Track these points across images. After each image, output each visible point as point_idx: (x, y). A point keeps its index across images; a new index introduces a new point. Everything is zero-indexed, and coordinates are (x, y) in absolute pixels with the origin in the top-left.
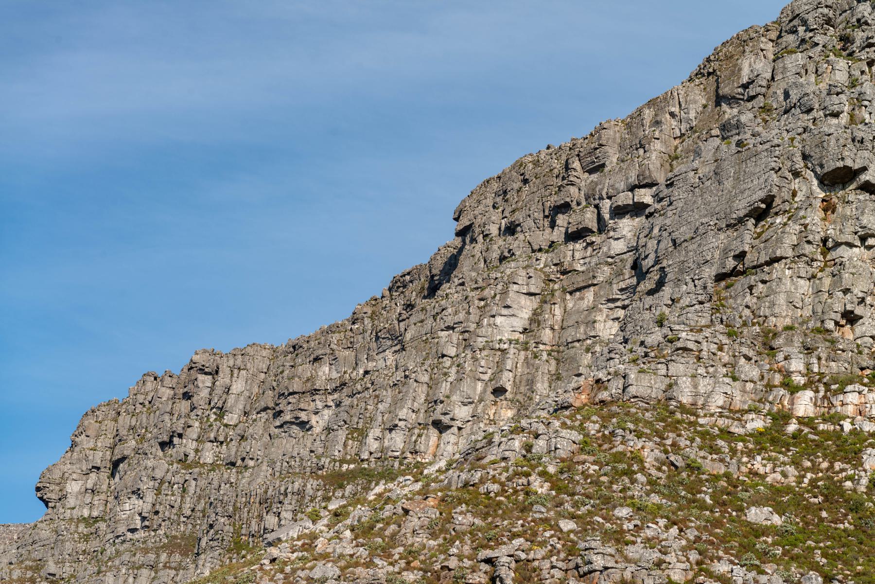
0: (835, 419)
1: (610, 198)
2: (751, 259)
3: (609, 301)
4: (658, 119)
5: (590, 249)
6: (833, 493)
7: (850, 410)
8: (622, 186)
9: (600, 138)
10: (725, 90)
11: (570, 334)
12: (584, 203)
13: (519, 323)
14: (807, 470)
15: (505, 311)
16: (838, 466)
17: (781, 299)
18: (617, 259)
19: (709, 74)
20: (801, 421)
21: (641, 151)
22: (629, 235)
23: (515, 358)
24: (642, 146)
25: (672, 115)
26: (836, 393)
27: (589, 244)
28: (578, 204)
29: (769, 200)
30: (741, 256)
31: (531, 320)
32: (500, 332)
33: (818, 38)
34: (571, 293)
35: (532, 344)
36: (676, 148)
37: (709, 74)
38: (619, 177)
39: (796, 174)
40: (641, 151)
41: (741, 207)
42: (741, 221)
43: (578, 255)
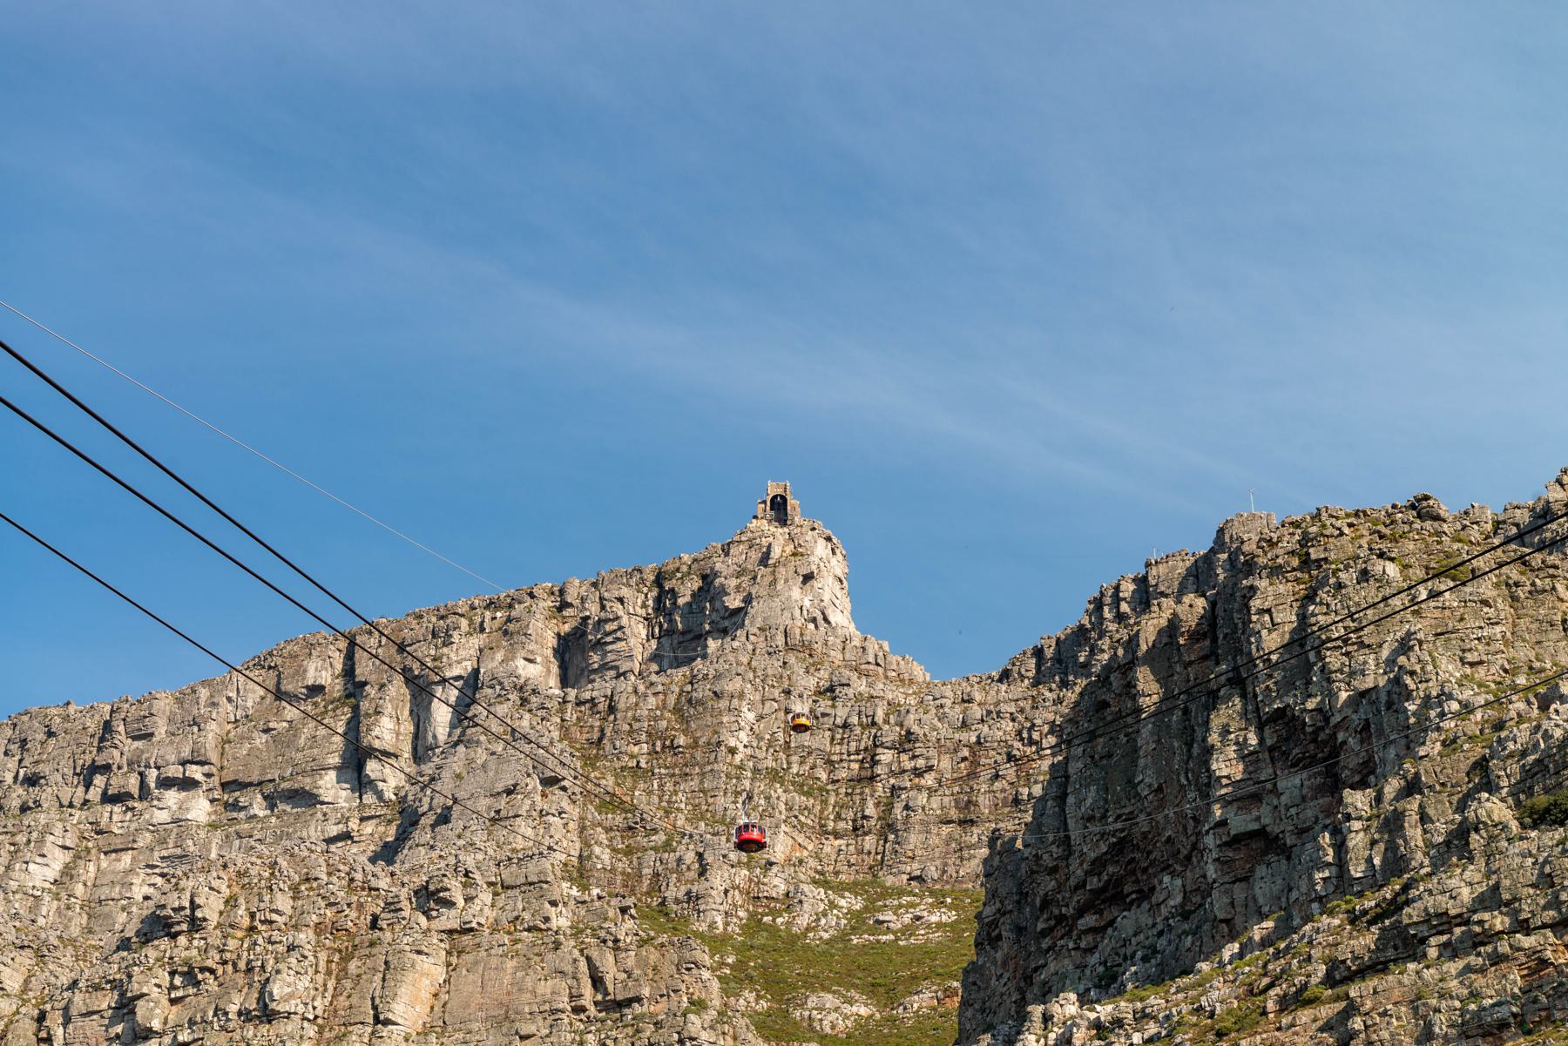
1: (158, 768)
2: (503, 814)
3: (148, 866)
5: (129, 814)
8: (173, 758)
9: (151, 706)
10: (288, 686)
11: (104, 892)
12: (125, 769)
13: (53, 872)
15: (39, 860)
18: (160, 828)
19: (270, 667)
21: (195, 729)
22: (174, 807)
23: (49, 906)
25: (229, 699)
27: (128, 809)
28: (119, 768)
29: (515, 786)
30: (498, 812)
31: (63, 873)
32: (32, 879)
34: (106, 853)
35: (63, 895)
37: (270, 667)
38: (169, 749)
40: (195, 729)
41: (500, 787)
43: (115, 818)
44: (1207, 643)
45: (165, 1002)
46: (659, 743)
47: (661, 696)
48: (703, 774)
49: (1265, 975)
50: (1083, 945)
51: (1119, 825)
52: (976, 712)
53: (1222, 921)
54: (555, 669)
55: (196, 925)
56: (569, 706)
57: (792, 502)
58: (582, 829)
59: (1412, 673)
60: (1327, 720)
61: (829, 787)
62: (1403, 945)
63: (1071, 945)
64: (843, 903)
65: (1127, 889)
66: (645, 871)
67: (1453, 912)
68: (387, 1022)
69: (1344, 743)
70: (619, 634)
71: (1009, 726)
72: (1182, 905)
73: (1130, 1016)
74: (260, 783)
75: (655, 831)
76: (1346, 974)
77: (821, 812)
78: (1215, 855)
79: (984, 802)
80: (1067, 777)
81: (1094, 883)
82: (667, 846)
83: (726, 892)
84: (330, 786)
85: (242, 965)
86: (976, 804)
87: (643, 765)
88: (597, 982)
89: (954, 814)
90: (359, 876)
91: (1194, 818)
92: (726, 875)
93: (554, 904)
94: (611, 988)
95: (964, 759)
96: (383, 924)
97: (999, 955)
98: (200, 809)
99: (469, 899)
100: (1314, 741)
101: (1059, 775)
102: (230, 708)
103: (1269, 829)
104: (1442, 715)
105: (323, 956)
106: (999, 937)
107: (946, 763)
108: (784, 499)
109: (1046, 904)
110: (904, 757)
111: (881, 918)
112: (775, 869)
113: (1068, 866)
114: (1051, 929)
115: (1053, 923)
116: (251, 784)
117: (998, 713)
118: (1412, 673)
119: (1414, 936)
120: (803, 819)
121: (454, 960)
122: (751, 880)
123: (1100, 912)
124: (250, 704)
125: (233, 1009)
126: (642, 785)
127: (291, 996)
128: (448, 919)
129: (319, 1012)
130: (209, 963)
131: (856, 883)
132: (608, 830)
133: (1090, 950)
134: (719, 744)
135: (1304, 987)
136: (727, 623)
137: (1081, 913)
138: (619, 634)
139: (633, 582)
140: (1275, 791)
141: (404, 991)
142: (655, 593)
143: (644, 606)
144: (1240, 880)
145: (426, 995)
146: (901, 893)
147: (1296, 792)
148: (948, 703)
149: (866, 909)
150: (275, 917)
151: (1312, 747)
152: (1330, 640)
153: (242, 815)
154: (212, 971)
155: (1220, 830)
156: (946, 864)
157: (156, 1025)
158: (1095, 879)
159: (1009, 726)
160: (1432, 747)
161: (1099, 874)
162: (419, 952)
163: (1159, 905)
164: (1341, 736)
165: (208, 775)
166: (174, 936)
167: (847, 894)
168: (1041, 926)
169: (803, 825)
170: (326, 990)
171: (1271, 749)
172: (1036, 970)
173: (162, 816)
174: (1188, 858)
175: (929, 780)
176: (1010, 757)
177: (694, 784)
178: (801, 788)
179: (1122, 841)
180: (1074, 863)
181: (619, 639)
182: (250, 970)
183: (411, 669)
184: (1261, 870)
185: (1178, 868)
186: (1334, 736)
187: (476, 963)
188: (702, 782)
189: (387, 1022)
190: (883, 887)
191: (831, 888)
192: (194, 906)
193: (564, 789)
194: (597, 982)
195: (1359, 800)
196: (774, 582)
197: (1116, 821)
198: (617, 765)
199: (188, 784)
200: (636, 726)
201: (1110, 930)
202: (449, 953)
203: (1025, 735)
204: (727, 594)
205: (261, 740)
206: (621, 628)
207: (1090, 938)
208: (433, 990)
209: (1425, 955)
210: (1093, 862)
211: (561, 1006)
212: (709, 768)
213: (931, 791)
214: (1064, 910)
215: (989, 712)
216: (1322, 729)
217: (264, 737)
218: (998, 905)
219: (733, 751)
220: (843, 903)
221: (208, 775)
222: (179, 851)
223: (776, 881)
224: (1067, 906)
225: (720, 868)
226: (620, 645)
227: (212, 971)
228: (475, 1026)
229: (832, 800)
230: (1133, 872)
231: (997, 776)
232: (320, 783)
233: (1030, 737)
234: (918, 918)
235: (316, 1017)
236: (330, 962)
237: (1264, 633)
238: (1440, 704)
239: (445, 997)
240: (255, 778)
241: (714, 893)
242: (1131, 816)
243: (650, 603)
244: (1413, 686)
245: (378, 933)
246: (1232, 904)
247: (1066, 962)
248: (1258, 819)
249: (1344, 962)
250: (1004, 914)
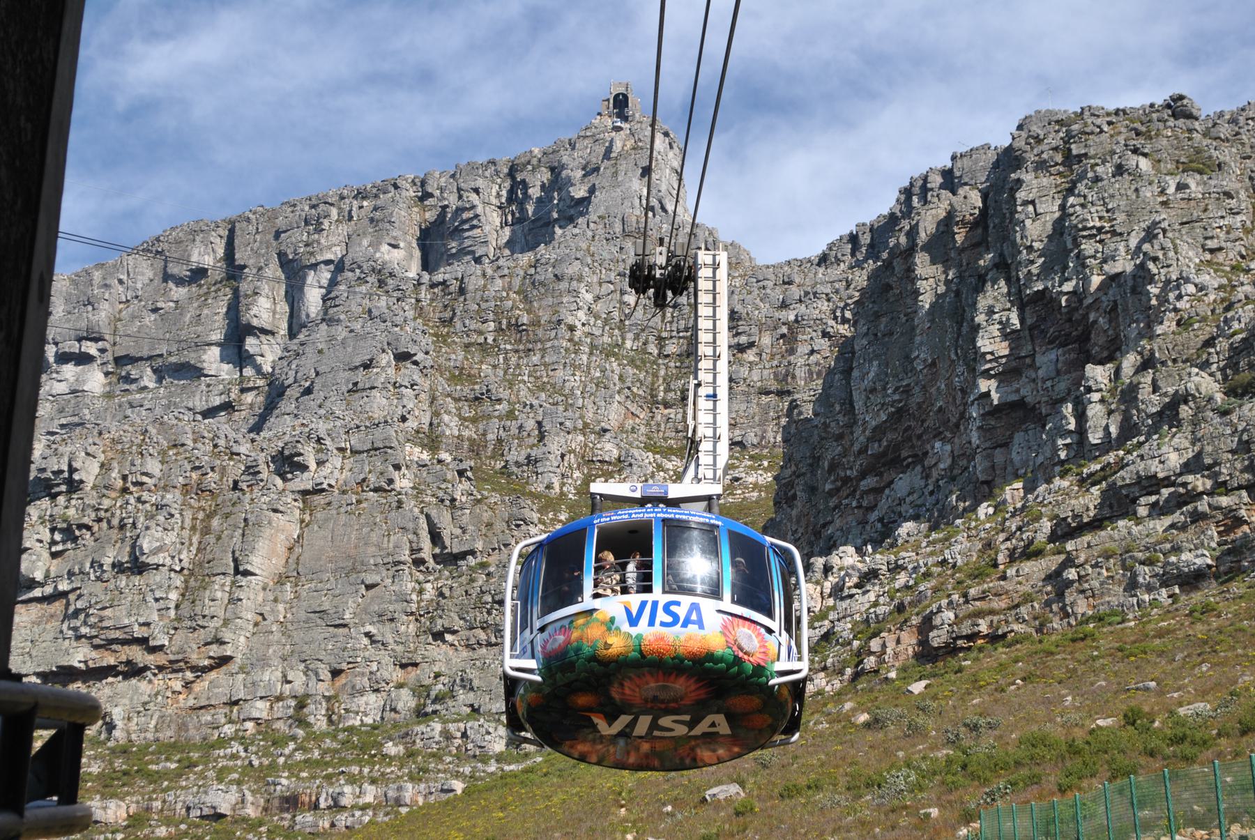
1: (56, 344)
2: (360, 386)
4: (108, 282)
10: (174, 269)
17: (375, 406)
21: (90, 308)
22: (72, 379)
24: (89, 303)
25: (121, 282)
29: (371, 360)
30: (355, 384)
33: (368, 279)
36: (120, 311)
37: (157, 252)
39: (384, 351)
40: (90, 308)
41: (357, 361)
42: (356, 368)
44: (980, 231)
45: (46, 555)
46: (504, 322)
47: (507, 279)
48: (544, 350)
49: (1003, 531)
50: (864, 504)
51: (897, 397)
52: (795, 292)
53: (983, 483)
54: (417, 253)
55: (74, 486)
56: (423, 288)
58: (433, 399)
59: (1155, 259)
60: (1081, 301)
61: (660, 361)
62: (1119, 504)
63: (854, 504)
64: (669, 465)
65: (904, 454)
66: (491, 437)
67: (1161, 475)
68: (247, 573)
69: (1095, 322)
70: (475, 222)
71: (824, 306)
72: (951, 468)
73: (885, 568)
74: (150, 358)
75: (499, 401)
76: (1066, 530)
77: (653, 384)
78: (978, 423)
79: (800, 373)
80: (853, 353)
81: (874, 448)
82: (510, 415)
83: (563, 456)
84: (211, 358)
85: (115, 522)
86: (794, 377)
87: (490, 340)
88: (436, 537)
90: (222, 442)
91: (962, 390)
92: (563, 441)
93: (397, 467)
94: (447, 542)
95: (783, 336)
96: (244, 486)
97: (794, 513)
98: (95, 380)
99: (320, 463)
100: (1070, 320)
101: (846, 350)
102: (121, 289)
103: (1028, 400)
104: (1179, 297)
105: (188, 515)
106: (794, 497)
107: (766, 340)
108: (626, 97)
109: (833, 467)
112: (608, 435)
113: (852, 433)
114: (838, 490)
115: (839, 484)
116: (141, 359)
117: (815, 294)
118: (1155, 259)
119: (1127, 496)
120: (635, 390)
121: (307, 518)
122: (586, 445)
123: (880, 474)
124: (139, 285)
125: (107, 562)
127: (159, 550)
128: (303, 481)
129: (185, 564)
130: (86, 520)
132: (457, 400)
133: (872, 508)
134: (559, 322)
135: (1031, 542)
136: (572, 212)
137: (863, 475)
138: (475, 222)
139: (487, 174)
140: (1033, 366)
141: (262, 546)
142: (507, 184)
143: (498, 196)
144: (1001, 446)
145: (281, 549)
147: (1052, 367)
148: (770, 284)
150: (145, 479)
151: (1067, 325)
152: (1085, 228)
153: (134, 387)
154: (89, 528)
155: (983, 401)
157: (39, 576)
158: (876, 445)
159: (824, 306)
160: (1167, 326)
161: (880, 441)
162: (276, 511)
163: (930, 468)
164: (1092, 317)
165: (102, 351)
166: (54, 497)
167: (673, 458)
168: (828, 487)
169: (635, 395)
170: (191, 544)
171: (1031, 328)
172: (825, 525)
173: (61, 388)
174: (957, 426)
176: (825, 334)
177: (535, 359)
178: (632, 362)
179: (899, 410)
180: (858, 431)
182: (122, 527)
183: (286, 254)
184: (1019, 437)
185: (949, 435)
186: (1086, 316)
187: (326, 520)
188: (543, 357)
189: (247, 573)
192: (72, 470)
193: (416, 363)
194: (436, 537)
195: (1098, 374)
196: (615, 174)
197: (894, 392)
198: (466, 340)
199: (83, 359)
200: (484, 305)
201: (887, 491)
202: (303, 510)
203: (838, 314)
204: (572, 185)
205: (150, 318)
206: (477, 216)
207: (871, 497)
208: (288, 545)
209: (1135, 513)
210: (875, 429)
211: (403, 558)
212: (549, 344)
214: (848, 473)
215: (807, 293)
216: (1077, 309)
217: (153, 317)
218: (793, 468)
219: (572, 328)
220: (669, 465)
221: (102, 351)
222: (76, 419)
223: (608, 446)
224: (851, 468)
225: (558, 434)
226: (476, 232)
227: (89, 528)
228: (325, 577)
229: (662, 373)
230: (910, 439)
231: (812, 352)
232: (204, 357)
233: (843, 316)
234: (737, 479)
235: (182, 569)
236: (194, 519)
237: (1028, 222)
238: (1178, 287)
239: (298, 550)
240: (145, 353)
241: (551, 457)
242: (907, 391)
243: (504, 193)
244: (1155, 271)
245: (238, 493)
246: (993, 467)
247: (850, 518)
248: (1018, 391)
249: (1065, 519)
250: (798, 477)
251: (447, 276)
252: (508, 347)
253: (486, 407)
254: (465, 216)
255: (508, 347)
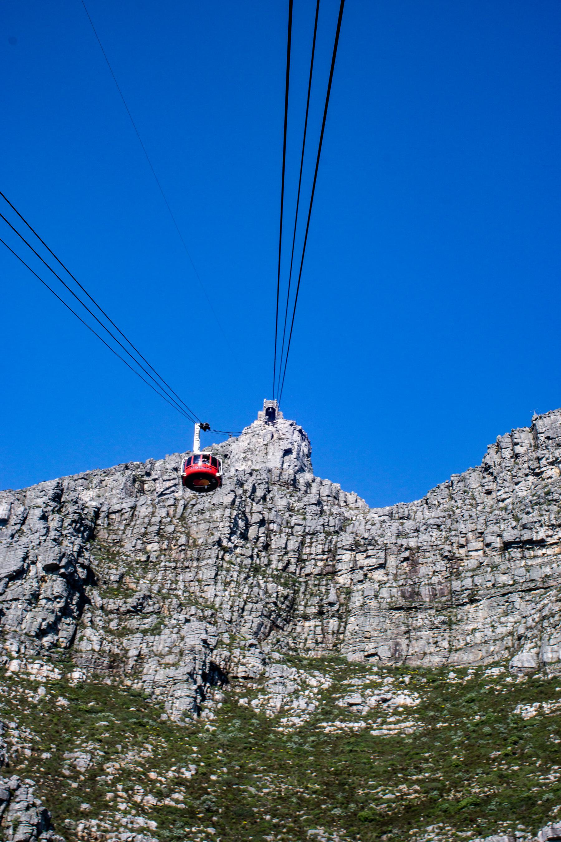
0: (29, 674)
6: (23, 701)
7: (34, 671)
14: (13, 691)
16: (27, 691)
20: (13, 672)
26: (30, 663)
57: (279, 414)
66: (133, 653)
79: (425, 592)
86: (418, 594)
87: (153, 558)
89: (402, 602)
95: (406, 559)
110: (360, 557)
111: (351, 701)
126: (150, 576)
131: (323, 659)
146: (362, 670)
149: (334, 688)
156: (397, 644)
167: (316, 673)
175: (379, 575)
177: (189, 575)
178: (277, 579)
181: (173, 492)
190: (344, 661)
191: (303, 667)
212: (204, 562)
213: (382, 584)
220: (313, 682)
234: (385, 701)
251: (124, 506)
252: (168, 564)
253: (134, 623)
254: (168, 484)
255: (168, 564)
